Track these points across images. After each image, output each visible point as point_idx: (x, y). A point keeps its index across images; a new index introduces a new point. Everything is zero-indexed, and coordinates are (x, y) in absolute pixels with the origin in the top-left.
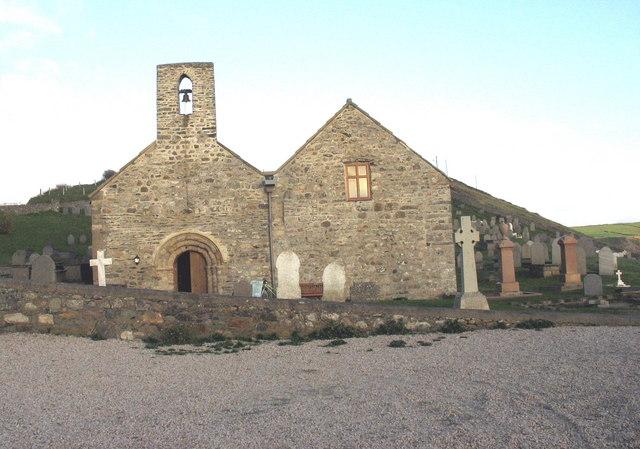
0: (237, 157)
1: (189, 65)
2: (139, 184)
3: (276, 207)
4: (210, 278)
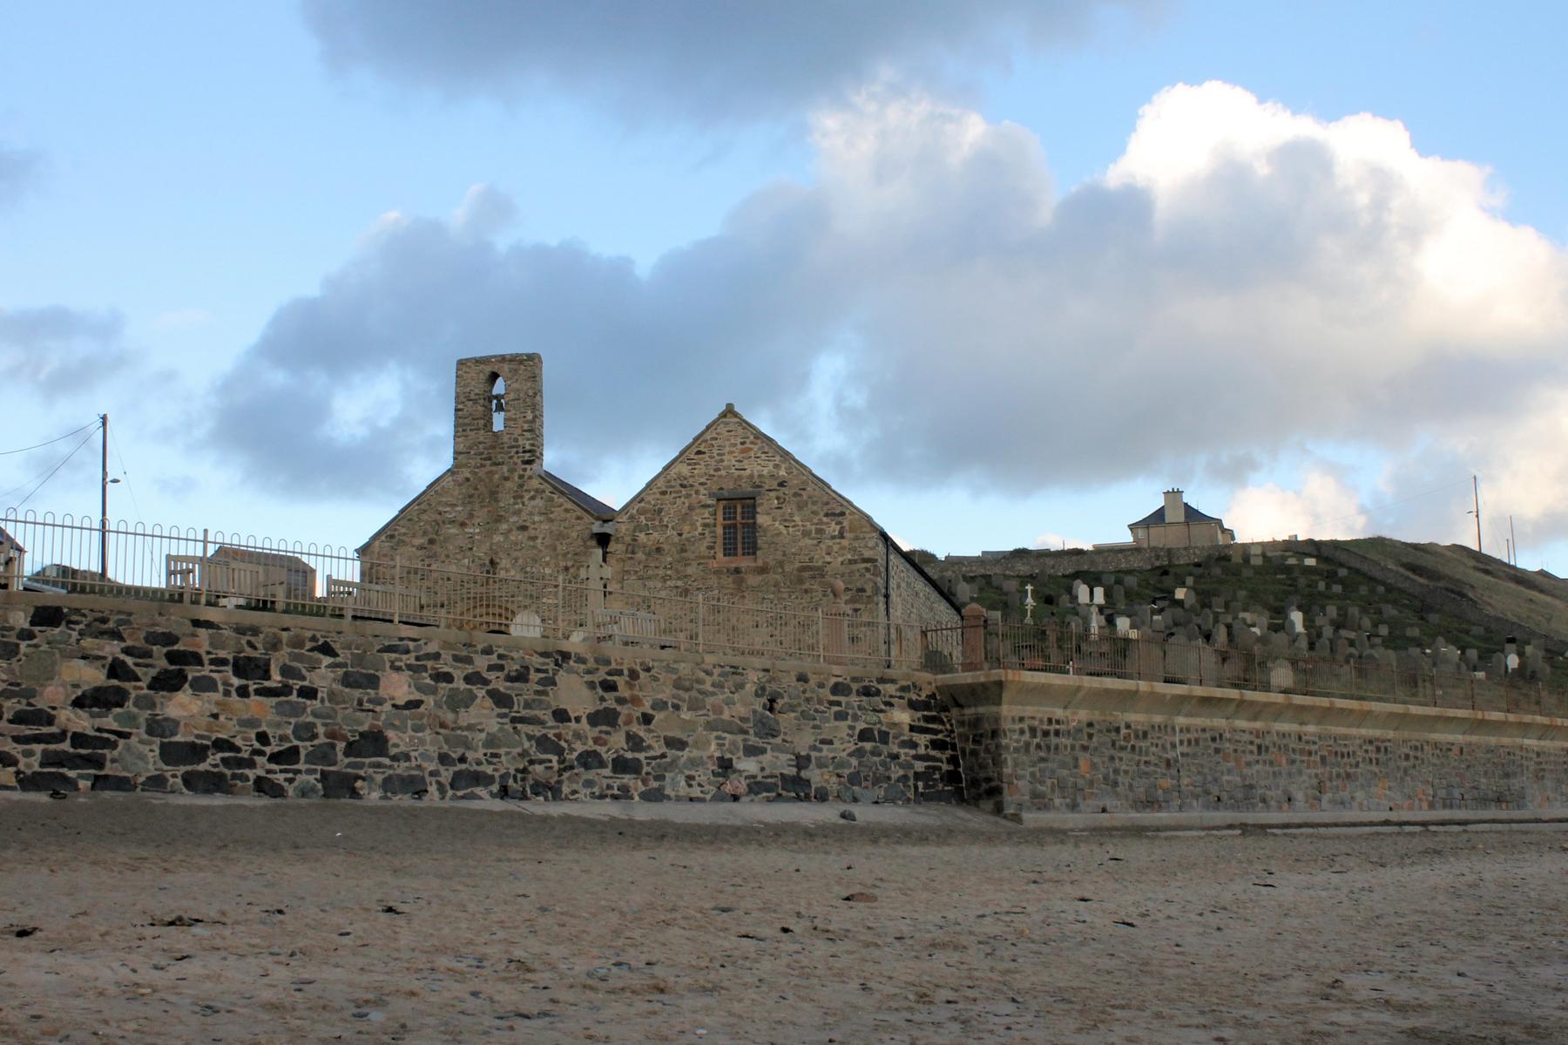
1: (503, 359)
2: (425, 533)
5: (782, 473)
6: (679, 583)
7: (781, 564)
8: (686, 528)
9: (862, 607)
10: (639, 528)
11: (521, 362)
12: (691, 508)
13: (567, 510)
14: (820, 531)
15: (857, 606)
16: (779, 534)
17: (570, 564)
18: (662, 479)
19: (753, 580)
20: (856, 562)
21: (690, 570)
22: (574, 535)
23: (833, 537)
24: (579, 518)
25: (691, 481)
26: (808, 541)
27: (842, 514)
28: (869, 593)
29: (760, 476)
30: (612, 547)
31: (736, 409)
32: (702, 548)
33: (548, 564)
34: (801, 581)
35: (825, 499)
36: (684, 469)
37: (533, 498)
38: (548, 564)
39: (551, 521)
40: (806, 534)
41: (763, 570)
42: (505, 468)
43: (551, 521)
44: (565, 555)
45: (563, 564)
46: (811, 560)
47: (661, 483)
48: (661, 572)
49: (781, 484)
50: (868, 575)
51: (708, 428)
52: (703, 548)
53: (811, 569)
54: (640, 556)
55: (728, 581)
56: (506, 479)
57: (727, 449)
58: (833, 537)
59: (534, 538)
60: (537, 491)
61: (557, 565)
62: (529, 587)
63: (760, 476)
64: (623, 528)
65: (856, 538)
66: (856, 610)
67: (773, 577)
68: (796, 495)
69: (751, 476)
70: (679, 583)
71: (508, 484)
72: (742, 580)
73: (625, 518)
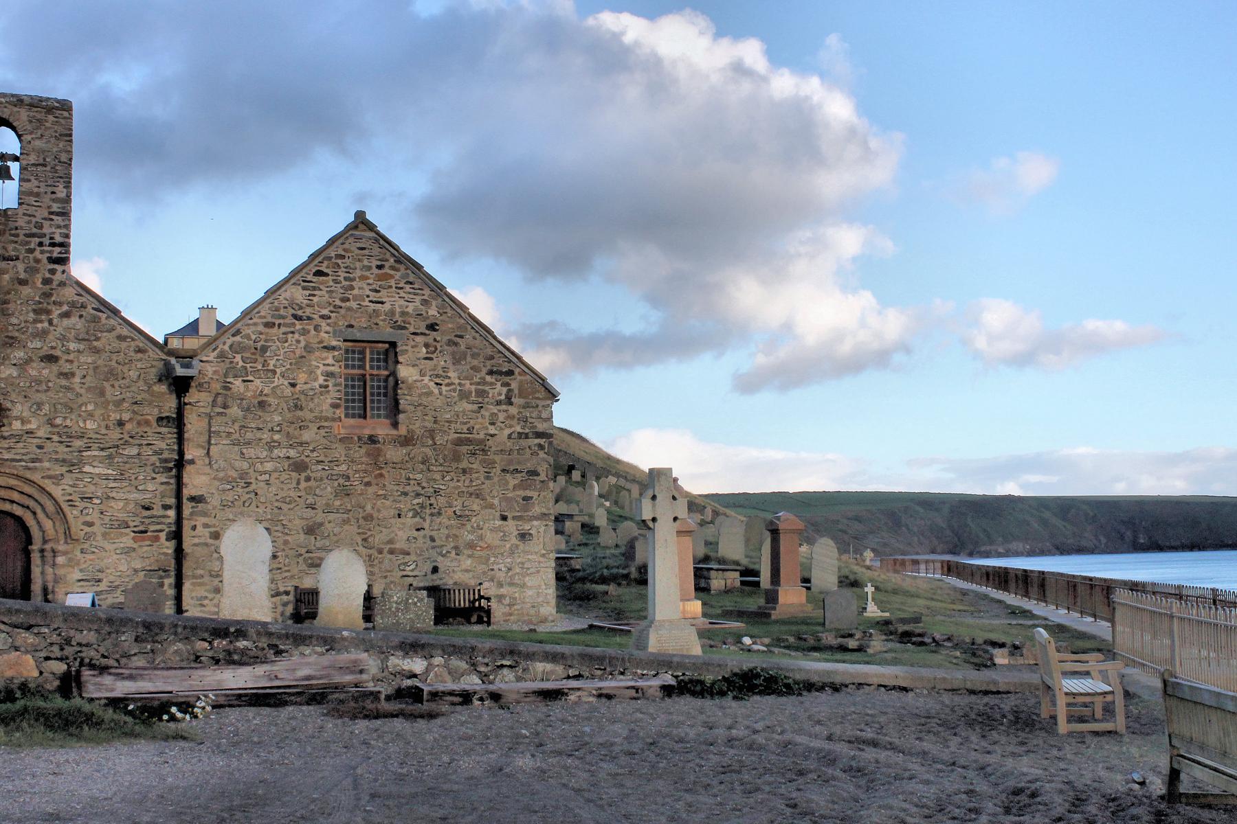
0: (116, 312)
3: (194, 425)
4: (36, 571)
5: (433, 312)
6: (292, 453)
7: (431, 433)
8: (302, 377)
9: (534, 494)
10: (232, 371)
11: (50, 110)
12: (308, 349)
13: (121, 338)
14: (481, 393)
15: (529, 493)
16: (430, 393)
17: (126, 416)
18: (266, 305)
19: (394, 453)
20: (527, 437)
21: (307, 436)
22: (133, 374)
23: (499, 403)
24: (140, 351)
25: (308, 311)
26: (465, 406)
27: (510, 373)
28: (543, 477)
29: (403, 314)
30: (192, 396)
31: (370, 217)
32: (325, 404)
33: (91, 415)
34: (457, 458)
35: (489, 351)
36: (299, 295)
37: (66, 315)
38: (91, 415)
39: (97, 351)
40: (464, 395)
41: (407, 441)
42: (21, 267)
43: (97, 351)
44: (118, 403)
45: (115, 416)
46: (470, 431)
47: (265, 309)
48: (266, 436)
49: (432, 327)
50: (542, 454)
51: (332, 241)
52: (326, 406)
53: (469, 442)
54: (235, 411)
55: (360, 453)
56: (23, 282)
57: (358, 273)
58: (499, 403)
59: (68, 375)
60: (73, 304)
61: (105, 418)
62: (62, 448)
63: (403, 314)
64: (210, 370)
65: (527, 406)
66: (526, 499)
67: (419, 451)
68: (451, 343)
69: (392, 313)
70: (292, 453)
71: (26, 291)
72: (378, 453)
73: (212, 356)
